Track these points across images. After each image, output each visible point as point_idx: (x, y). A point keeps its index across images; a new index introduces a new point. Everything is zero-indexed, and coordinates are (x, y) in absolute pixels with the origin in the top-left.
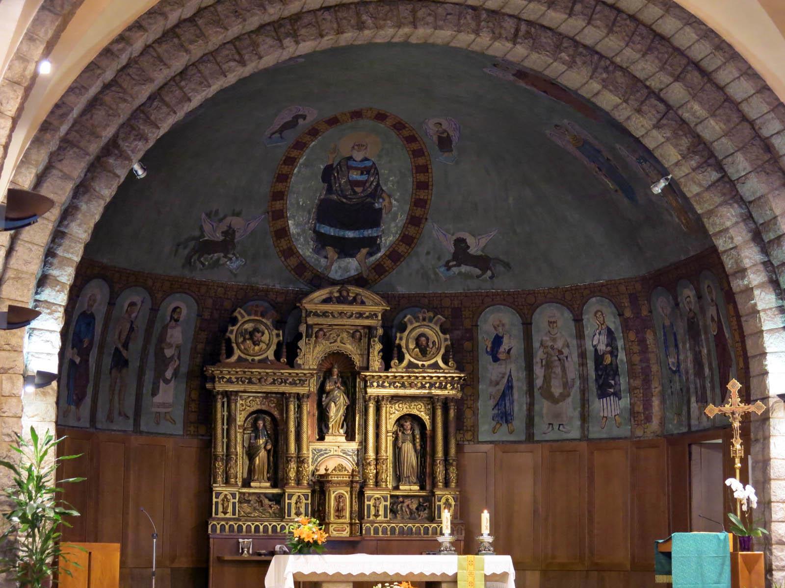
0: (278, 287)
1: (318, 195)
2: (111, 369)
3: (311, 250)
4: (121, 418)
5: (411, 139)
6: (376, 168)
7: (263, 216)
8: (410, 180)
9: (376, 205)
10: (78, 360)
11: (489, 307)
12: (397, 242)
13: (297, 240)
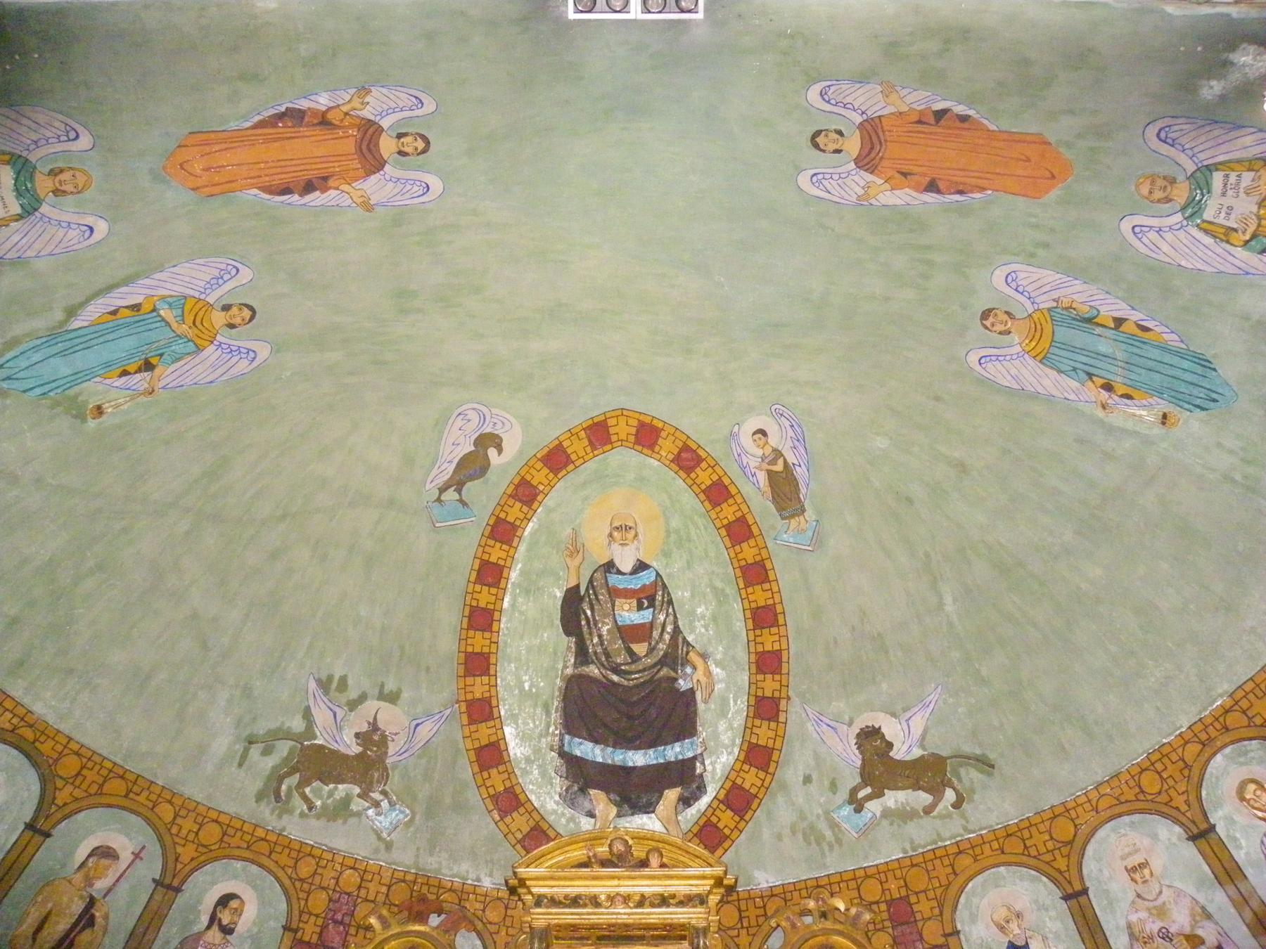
0: (487, 883)
1: (560, 666)
3: (557, 798)
5: (717, 493)
6: (664, 587)
7: (449, 710)
8: (737, 607)
9: (681, 682)
11: (970, 879)
12: (738, 767)
13: (526, 772)
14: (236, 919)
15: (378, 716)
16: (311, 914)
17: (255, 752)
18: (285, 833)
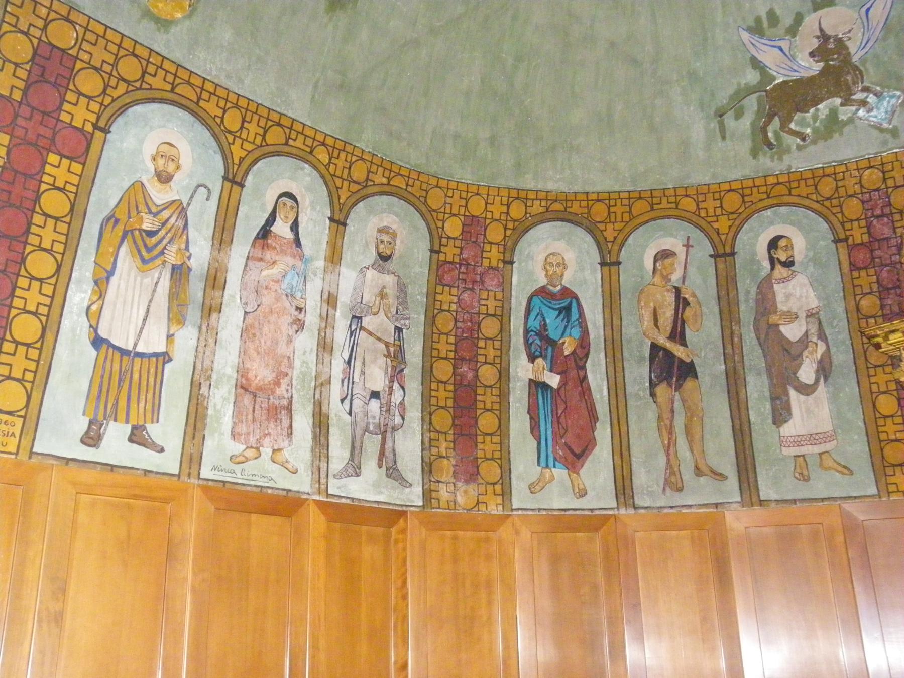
2: (652, 385)
4: (702, 479)
10: (554, 381)
14: (790, 253)
15: (823, 26)
16: (852, 221)
17: (730, 121)
18: (793, 170)
